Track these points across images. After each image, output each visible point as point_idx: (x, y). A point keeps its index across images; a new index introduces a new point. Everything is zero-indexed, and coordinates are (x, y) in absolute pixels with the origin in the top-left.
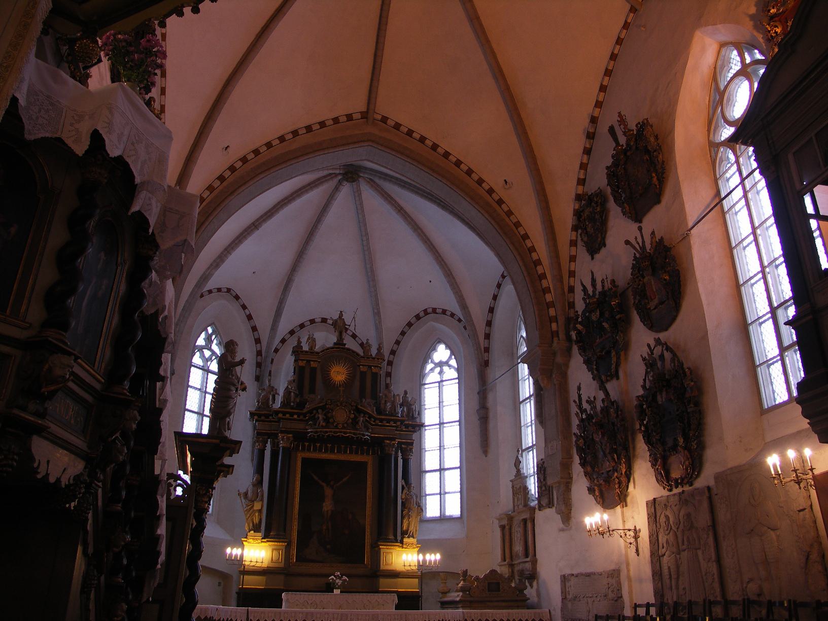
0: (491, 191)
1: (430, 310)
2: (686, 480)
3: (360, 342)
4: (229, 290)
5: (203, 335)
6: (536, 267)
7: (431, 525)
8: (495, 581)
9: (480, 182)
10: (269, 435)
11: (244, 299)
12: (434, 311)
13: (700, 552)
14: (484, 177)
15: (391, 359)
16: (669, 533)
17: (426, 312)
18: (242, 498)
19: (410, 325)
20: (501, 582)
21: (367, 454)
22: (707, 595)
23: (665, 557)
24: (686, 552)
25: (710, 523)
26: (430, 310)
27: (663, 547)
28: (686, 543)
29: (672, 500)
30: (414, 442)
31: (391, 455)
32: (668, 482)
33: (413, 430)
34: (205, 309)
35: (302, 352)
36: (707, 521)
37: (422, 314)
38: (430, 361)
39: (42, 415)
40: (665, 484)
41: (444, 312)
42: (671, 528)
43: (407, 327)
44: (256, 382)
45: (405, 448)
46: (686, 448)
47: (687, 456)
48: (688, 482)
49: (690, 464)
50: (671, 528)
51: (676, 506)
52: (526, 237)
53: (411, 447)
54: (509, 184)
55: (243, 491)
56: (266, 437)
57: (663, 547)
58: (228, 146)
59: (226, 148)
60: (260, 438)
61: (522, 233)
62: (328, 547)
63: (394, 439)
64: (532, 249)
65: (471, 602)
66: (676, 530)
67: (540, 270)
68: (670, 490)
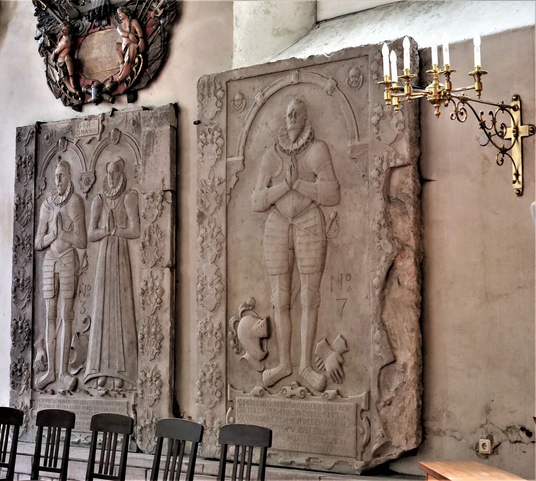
2: (123, 88)
13: (135, 247)
16: (66, 201)
22: (139, 336)
23: (48, 252)
24: (102, 243)
25: (168, 185)
27: (47, 232)
28: (104, 223)
29: (82, 128)
32: (78, 87)
36: (163, 181)
40: (71, 94)
42: (72, 191)
46: (132, 15)
47: (136, 32)
48: (127, 92)
49: (138, 53)
50: (72, 191)
51: (89, 142)
57: (47, 232)
66: (84, 196)
68: (79, 108)
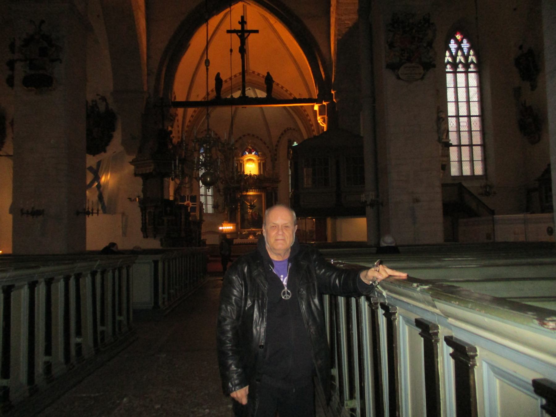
1: (289, 128)
19: (282, 134)
26: (289, 128)
64: (310, 120)
67: (313, 128)
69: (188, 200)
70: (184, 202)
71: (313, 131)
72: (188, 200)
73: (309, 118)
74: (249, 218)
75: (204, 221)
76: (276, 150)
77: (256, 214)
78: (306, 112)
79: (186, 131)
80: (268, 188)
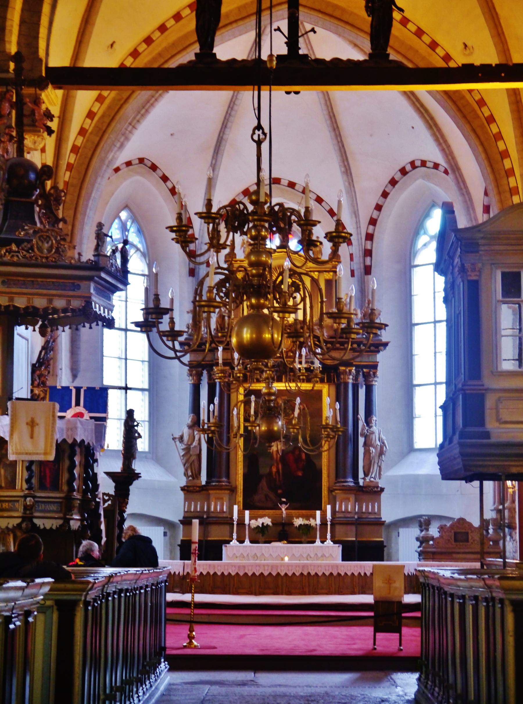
0: (447, 58)
1: (418, 163)
3: (328, 208)
4: (141, 161)
5: (116, 224)
6: (502, 159)
7: (423, 456)
8: (464, 531)
9: (434, 45)
10: (204, 367)
11: (164, 168)
12: (424, 163)
14: (438, 40)
15: (370, 231)
17: (413, 164)
18: (178, 443)
19: (393, 182)
20: (470, 531)
21: (322, 381)
26: (418, 163)
30: (379, 365)
31: (346, 384)
33: (376, 349)
34: (113, 194)
35: (236, 261)
37: (408, 168)
38: (422, 232)
39: (72, 515)
41: (436, 166)
43: (389, 185)
44: (191, 278)
45: (367, 372)
52: (491, 119)
53: (374, 371)
54: (469, 49)
55: (177, 435)
56: (200, 369)
58: (114, 42)
59: (112, 45)
60: (192, 371)
61: (487, 114)
62: (280, 491)
63: (351, 365)
64: (499, 136)
65: (434, 553)
67: (507, 163)
69: (78, 404)
70: (66, 412)
71: (510, 173)
72: (78, 404)
73: (494, 129)
74: (274, 469)
75: (137, 476)
76: (370, 237)
77: (300, 455)
78: (485, 109)
79: (70, 167)
80: (342, 368)
